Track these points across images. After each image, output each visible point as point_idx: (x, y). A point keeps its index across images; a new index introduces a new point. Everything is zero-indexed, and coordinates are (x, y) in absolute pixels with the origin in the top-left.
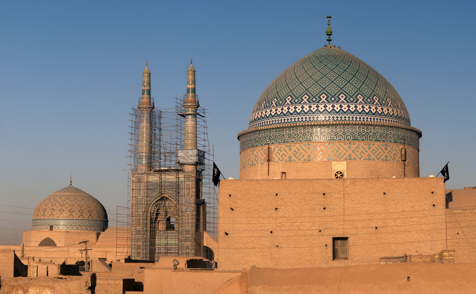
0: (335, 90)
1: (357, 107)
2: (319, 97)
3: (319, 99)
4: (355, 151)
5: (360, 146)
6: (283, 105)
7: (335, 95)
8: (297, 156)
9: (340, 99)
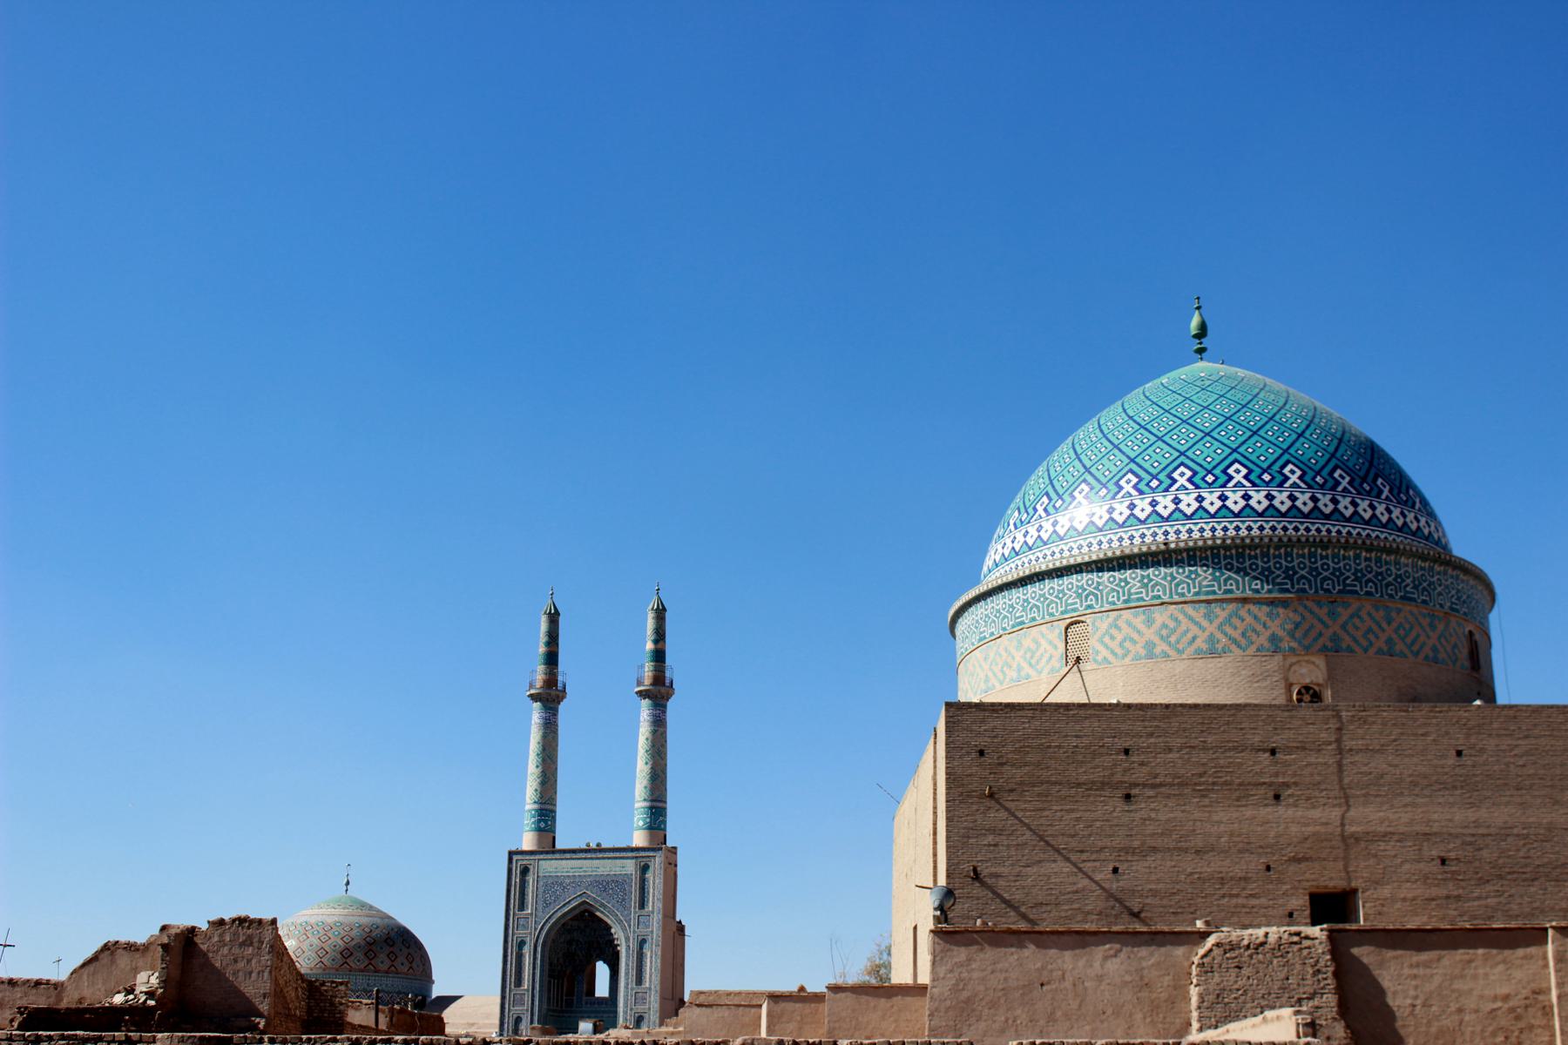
2: (1224, 471)
3: (1223, 478)
4: (1350, 627)
6: (1113, 498)
8: (1173, 639)
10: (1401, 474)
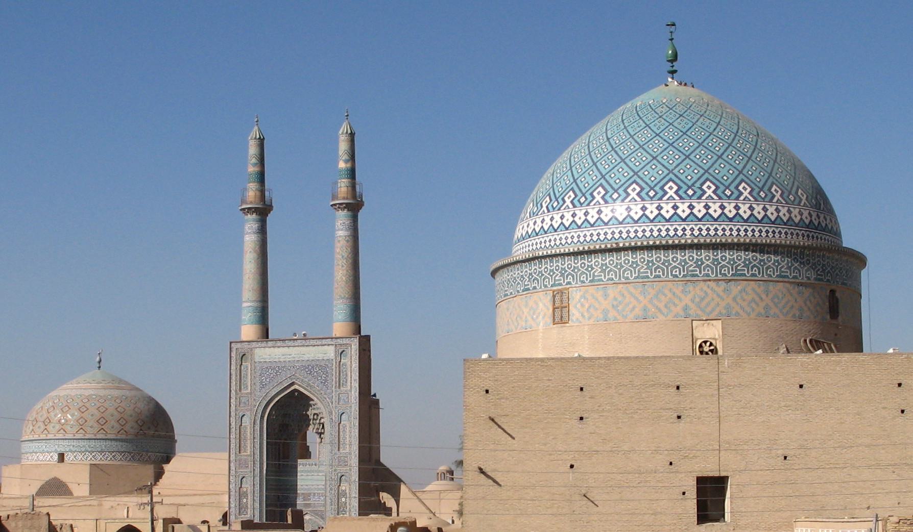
0: (693, 175)
1: (739, 208)
2: (662, 188)
3: (661, 193)
4: (738, 299)
9: (705, 192)
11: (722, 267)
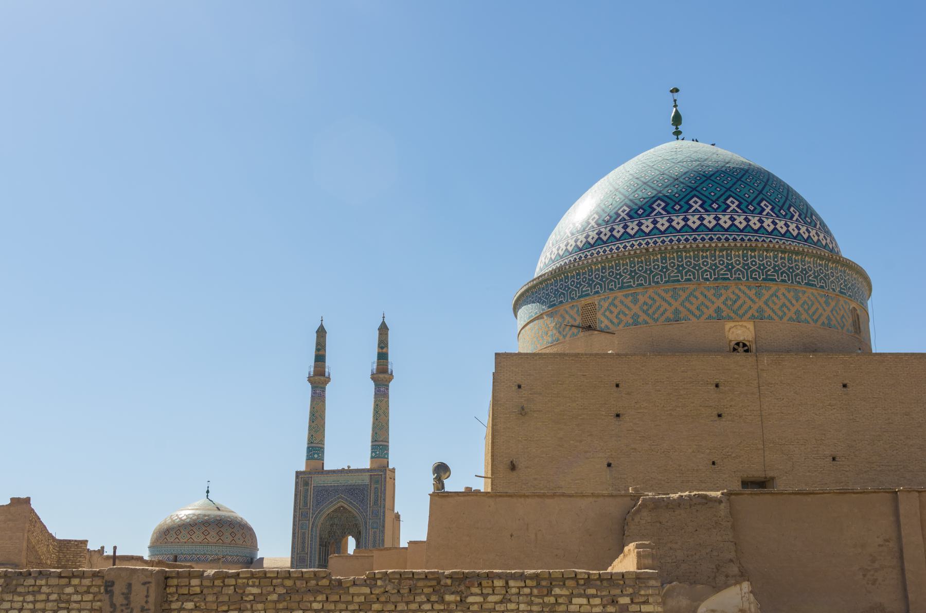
1: (763, 222)
2: (687, 203)
4: (770, 303)
5: (780, 294)
7: (717, 200)
8: (650, 312)
10: (808, 207)
11: (752, 272)
